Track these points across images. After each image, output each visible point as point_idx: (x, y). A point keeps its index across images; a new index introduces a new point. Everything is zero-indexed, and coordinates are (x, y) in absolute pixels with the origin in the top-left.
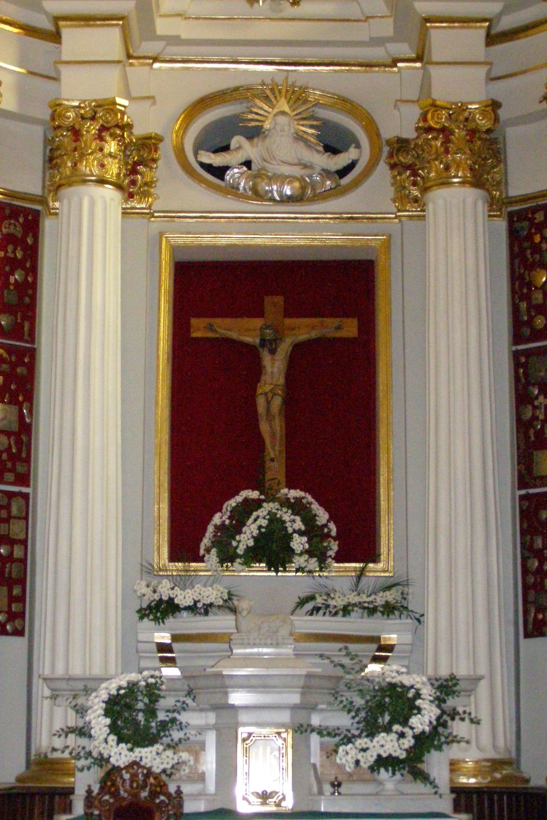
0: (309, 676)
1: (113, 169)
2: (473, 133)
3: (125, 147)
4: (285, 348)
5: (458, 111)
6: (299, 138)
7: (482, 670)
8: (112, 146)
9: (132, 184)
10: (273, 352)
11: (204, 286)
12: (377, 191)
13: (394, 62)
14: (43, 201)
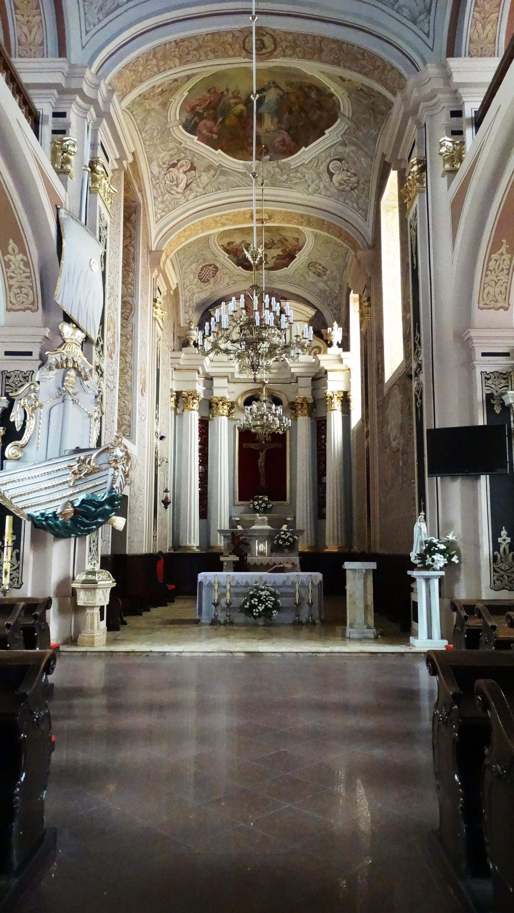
1: (226, 412)
2: (308, 404)
3: (228, 406)
4: (264, 452)
5: (304, 399)
7: (305, 528)
8: (225, 407)
9: (229, 414)
11: (246, 436)
13: (291, 383)
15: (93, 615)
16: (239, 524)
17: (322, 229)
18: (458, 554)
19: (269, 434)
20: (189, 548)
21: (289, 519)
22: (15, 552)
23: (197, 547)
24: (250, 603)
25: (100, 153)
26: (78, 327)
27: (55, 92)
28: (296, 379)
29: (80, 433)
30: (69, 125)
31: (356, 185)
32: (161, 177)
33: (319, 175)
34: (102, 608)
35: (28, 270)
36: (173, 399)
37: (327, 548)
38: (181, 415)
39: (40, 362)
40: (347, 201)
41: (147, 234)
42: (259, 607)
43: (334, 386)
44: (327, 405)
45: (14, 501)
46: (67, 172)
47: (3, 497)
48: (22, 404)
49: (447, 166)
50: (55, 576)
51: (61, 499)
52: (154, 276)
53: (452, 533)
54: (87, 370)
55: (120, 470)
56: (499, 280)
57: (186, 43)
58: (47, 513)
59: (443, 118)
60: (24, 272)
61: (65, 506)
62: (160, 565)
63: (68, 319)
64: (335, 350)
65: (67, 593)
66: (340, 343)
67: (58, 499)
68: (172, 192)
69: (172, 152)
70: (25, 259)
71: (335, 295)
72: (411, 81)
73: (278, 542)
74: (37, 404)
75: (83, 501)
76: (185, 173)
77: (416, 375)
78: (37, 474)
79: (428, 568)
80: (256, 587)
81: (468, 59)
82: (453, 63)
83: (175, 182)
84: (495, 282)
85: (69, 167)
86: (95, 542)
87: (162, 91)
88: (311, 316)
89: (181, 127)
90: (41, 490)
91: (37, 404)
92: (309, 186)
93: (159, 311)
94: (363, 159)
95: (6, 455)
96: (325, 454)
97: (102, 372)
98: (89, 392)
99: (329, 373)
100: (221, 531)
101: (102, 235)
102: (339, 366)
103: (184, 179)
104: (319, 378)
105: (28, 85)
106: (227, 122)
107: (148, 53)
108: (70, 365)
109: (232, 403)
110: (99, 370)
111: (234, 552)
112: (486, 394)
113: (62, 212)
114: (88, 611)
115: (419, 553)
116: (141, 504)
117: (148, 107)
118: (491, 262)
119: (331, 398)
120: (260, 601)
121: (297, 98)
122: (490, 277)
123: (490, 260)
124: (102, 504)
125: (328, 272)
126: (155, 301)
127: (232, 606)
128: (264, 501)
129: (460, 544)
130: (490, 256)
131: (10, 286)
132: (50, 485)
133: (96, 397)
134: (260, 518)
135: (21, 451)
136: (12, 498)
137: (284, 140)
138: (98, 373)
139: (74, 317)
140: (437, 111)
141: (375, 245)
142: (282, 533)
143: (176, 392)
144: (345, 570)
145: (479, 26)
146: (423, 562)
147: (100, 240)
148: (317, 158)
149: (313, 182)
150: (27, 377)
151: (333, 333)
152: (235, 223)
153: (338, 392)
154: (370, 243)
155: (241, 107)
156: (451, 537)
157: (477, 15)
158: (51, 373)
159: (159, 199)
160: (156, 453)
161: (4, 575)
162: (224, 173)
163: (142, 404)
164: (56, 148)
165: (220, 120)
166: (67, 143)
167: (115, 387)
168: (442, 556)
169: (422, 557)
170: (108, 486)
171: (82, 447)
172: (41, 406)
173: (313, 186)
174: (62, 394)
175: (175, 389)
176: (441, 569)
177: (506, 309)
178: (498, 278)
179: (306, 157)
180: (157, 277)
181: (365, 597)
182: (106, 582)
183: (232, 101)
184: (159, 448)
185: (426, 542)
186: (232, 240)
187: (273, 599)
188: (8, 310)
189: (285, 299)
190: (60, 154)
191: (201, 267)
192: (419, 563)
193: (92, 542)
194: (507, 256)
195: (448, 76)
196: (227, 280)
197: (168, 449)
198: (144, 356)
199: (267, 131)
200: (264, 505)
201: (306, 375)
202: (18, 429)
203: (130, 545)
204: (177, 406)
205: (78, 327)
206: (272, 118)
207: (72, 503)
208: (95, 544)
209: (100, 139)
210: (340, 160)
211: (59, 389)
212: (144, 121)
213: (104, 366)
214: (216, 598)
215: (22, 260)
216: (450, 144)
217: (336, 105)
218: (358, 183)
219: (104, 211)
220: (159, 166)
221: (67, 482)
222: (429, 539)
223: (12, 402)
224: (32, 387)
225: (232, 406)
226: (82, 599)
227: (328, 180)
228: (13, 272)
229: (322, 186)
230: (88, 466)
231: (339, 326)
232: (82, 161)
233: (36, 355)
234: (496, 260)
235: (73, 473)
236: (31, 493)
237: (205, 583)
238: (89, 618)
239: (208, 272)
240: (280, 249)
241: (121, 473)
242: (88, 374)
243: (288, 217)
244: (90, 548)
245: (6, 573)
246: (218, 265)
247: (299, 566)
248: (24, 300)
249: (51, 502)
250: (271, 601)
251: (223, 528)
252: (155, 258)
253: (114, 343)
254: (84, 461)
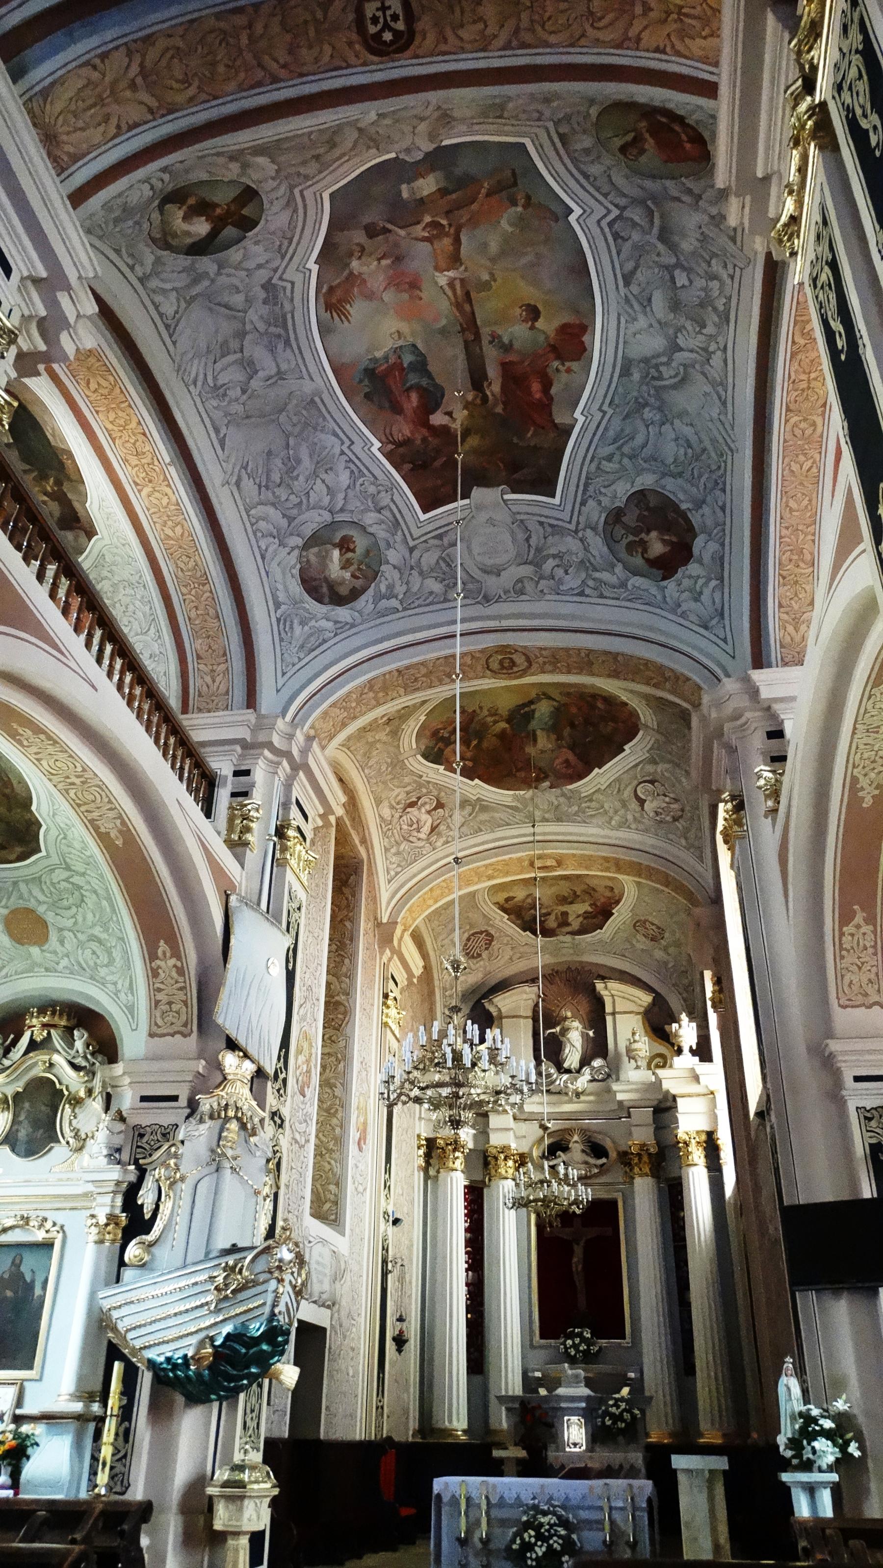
0: (588, 1399)
1: (511, 1171)
2: (650, 1155)
3: (515, 1162)
4: (582, 1243)
5: (643, 1146)
6: (583, 1151)
8: (510, 1163)
10: (578, 1244)
12: (617, 1175)
14: (483, 1182)
15: (237, 1550)
16: (542, 1386)
17: (640, 876)
18: (860, 1439)
19: (557, 1215)
20: (449, 1432)
21: (632, 1375)
22: (123, 1426)
23: (464, 1431)
24: (522, 1539)
25: (294, 812)
26: (246, 1056)
27: (238, 748)
28: (625, 1110)
29: (240, 1220)
30: (253, 785)
31: (680, 813)
32: (395, 820)
33: (624, 804)
34: (256, 1538)
35: (181, 979)
36: (421, 1152)
37: (701, 1435)
38: (436, 1178)
39: (188, 1111)
40: (671, 836)
41: (374, 899)
42: (537, 1549)
43: (690, 1121)
44: (680, 1157)
45: (130, 1336)
46: (246, 844)
47: (114, 1329)
48: (157, 1176)
49: (770, 803)
50: (182, 1473)
51: (196, 1332)
52: (385, 959)
53: (844, 1397)
54: (256, 1120)
55: (286, 1283)
56: (863, 963)
57: (412, 671)
58: (176, 1356)
59: (758, 741)
60: (177, 982)
61: (201, 1344)
62: (388, 1463)
63: (232, 1045)
64: (686, 1061)
65: (197, 1506)
66: (694, 1047)
67: (192, 1334)
68: (411, 839)
69: (409, 788)
70: (179, 964)
71: (683, 969)
72: (706, 699)
73: (603, 1422)
74: (178, 1175)
75: (228, 1334)
76: (429, 812)
77: (768, 1114)
78: (163, 1291)
79: (807, 1466)
80: (535, 1507)
81: (780, 669)
82: (757, 676)
83: (415, 826)
85: (249, 837)
86: (253, 1411)
87: (389, 720)
88: (645, 1004)
89: (419, 757)
90: (169, 1317)
91: (178, 1175)
92: (611, 818)
93: (393, 1012)
94: (684, 780)
95: (126, 1259)
96: (685, 1247)
97: (283, 1121)
98: (258, 1154)
99: (679, 1100)
100: (501, 1399)
101: (292, 920)
102: (694, 1088)
103: (427, 821)
104: (664, 1109)
105: (204, 744)
106: (485, 745)
107: (362, 687)
108: (231, 1113)
109: (522, 1156)
110: (276, 1119)
111: (522, 1442)
112: (870, 1145)
113: (233, 898)
114: (231, 1542)
115: (790, 1435)
116: (353, 1345)
117: (370, 740)
118: (844, 938)
119: (687, 1144)
120: (539, 1536)
121: (579, 709)
122: (848, 960)
123: (842, 934)
124: (257, 1341)
125: (667, 935)
126: (386, 996)
127: (492, 1546)
128: (583, 1340)
129: (861, 1420)
130: (840, 929)
131: (157, 1002)
132: (182, 1308)
133: (268, 1161)
134: (570, 1372)
135: (149, 1253)
136: (128, 1331)
137: (567, 761)
138: (275, 1122)
139: (242, 1041)
140: (750, 732)
141: (717, 900)
142: (611, 1402)
143: (427, 1140)
144: (675, 1471)
145: (790, 629)
146: (799, 1455)
147: (288, 930)
148: (618, 780)
149: (616, 812)
150: (167, 1133)
151: (681, 1032)
152: (507, 874)
153: (698, 1132)
154: (713, 895)
155: (503, 725)
156: (840, 1405)
157: (785, 617)
158: (203, 1128)
159: (393, 850)
160: (385, 1249)
161: (100, 1467)
162: (484, 809)
163: (360, 1165)
164: (234, 815)
165: (475, 742)
166: (249, 807)
167: (308, 1141)
168: (829, 1443)
169: (795, 1444)
170: (267, 1310)
171: (240, 1245)
172: (183, 1179)
173: (617, 818)
174: (216, 1160)
175: (424, 1135)
176: (830, 1469)
179: (602, 781)
180: (390, 960)
181: (714, 1530)
182: (263, 1486)
183: (489, 719)
184: (390, 1241)
185: (801, 1415)
186: (511, 894)
187: (563, 1532)
188: (151, 1035)
189: (603, 978)
190: (238, 821)
191: (466, 935)
192: (793, 1457)
193: (248, 1411)
194: (867, 929)
195: (754, 692)
196: (508, 953)
197: (411, 1240)
198: (365, 1085)
199: (542, 752)
200: (583, 1347)
201: (643, 1104)
202: (147, 1216)
203: (329, 1424)
204: (428, 1164)
205: (246, 1056)
206: (548, 737)
207: (212, 1339)
208: (254, 1415)
209: (295, 794)
210: (652, 782)
211: (213, 1151)
212: (367, 756)
213: (285, 1112)
214: (463, 1527)
215: (175, 966)
216: (770, 775)
217: (634, 714)
218: (682, 810)
219: (296, 886)
220: (392, 807)
221: (207, 1303)
222: (803, 1408)
223: (142, 1173)
224: (173, 1149)
225: (522, 1160)
226: (222, 1519)
227: (638, 809)
228: (162, 983)
229: (630, 817)
230: (239, 1277)
231: (691, 1020)
232: (267, 828)
233: (183, 1101)
234: (852, 935)
235: (217, 1288)
236: (155, 1321)
237: (446, 1499)
238: (230, 1555)
239: (480, 941)
240: (587, 904)
241: (289, 1288)
242: (258, 1126)
243: (587, 861)
244: (245, 1423)
245: (104, 1464)
246: (493, 932)
247: (643, 1470)
248: (174, 1020)
249: (181, 1337)
250: (560, 1537)
251: (510, 1393)
252: (385, 934)
253: (309, 1071)
254: (233, 1269)
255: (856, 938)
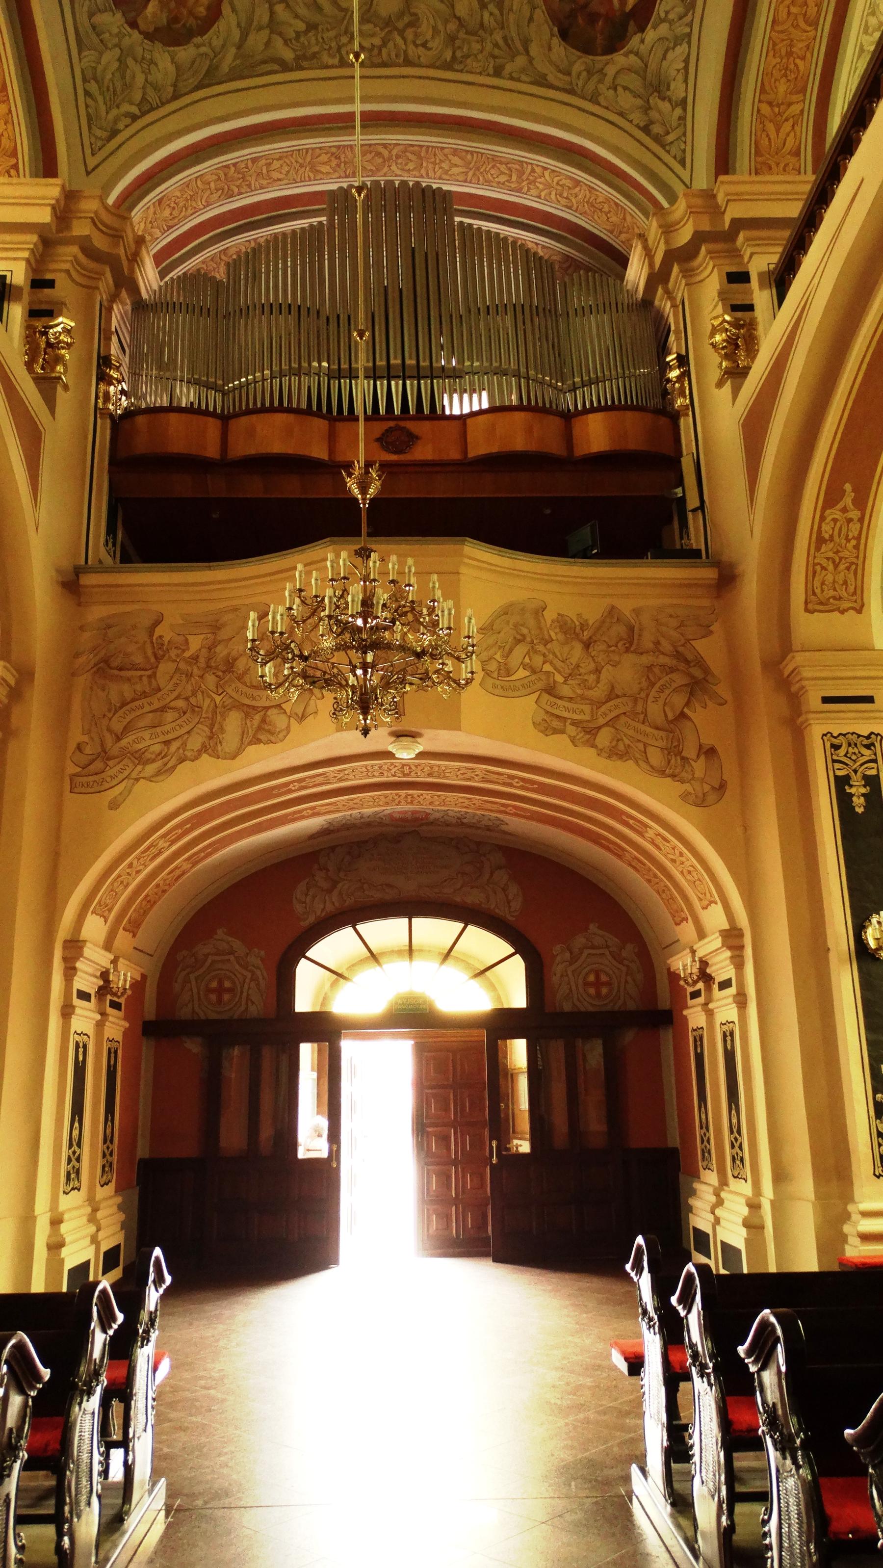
84: (834, 562)
177: (859, 611)
178: (841, 554)
194: (855, 514)
234: (835, 520)
255: (838, 524)
